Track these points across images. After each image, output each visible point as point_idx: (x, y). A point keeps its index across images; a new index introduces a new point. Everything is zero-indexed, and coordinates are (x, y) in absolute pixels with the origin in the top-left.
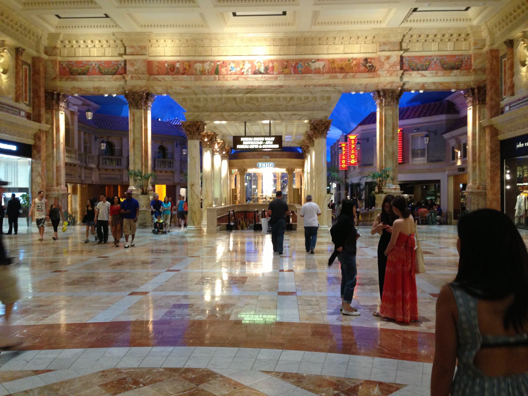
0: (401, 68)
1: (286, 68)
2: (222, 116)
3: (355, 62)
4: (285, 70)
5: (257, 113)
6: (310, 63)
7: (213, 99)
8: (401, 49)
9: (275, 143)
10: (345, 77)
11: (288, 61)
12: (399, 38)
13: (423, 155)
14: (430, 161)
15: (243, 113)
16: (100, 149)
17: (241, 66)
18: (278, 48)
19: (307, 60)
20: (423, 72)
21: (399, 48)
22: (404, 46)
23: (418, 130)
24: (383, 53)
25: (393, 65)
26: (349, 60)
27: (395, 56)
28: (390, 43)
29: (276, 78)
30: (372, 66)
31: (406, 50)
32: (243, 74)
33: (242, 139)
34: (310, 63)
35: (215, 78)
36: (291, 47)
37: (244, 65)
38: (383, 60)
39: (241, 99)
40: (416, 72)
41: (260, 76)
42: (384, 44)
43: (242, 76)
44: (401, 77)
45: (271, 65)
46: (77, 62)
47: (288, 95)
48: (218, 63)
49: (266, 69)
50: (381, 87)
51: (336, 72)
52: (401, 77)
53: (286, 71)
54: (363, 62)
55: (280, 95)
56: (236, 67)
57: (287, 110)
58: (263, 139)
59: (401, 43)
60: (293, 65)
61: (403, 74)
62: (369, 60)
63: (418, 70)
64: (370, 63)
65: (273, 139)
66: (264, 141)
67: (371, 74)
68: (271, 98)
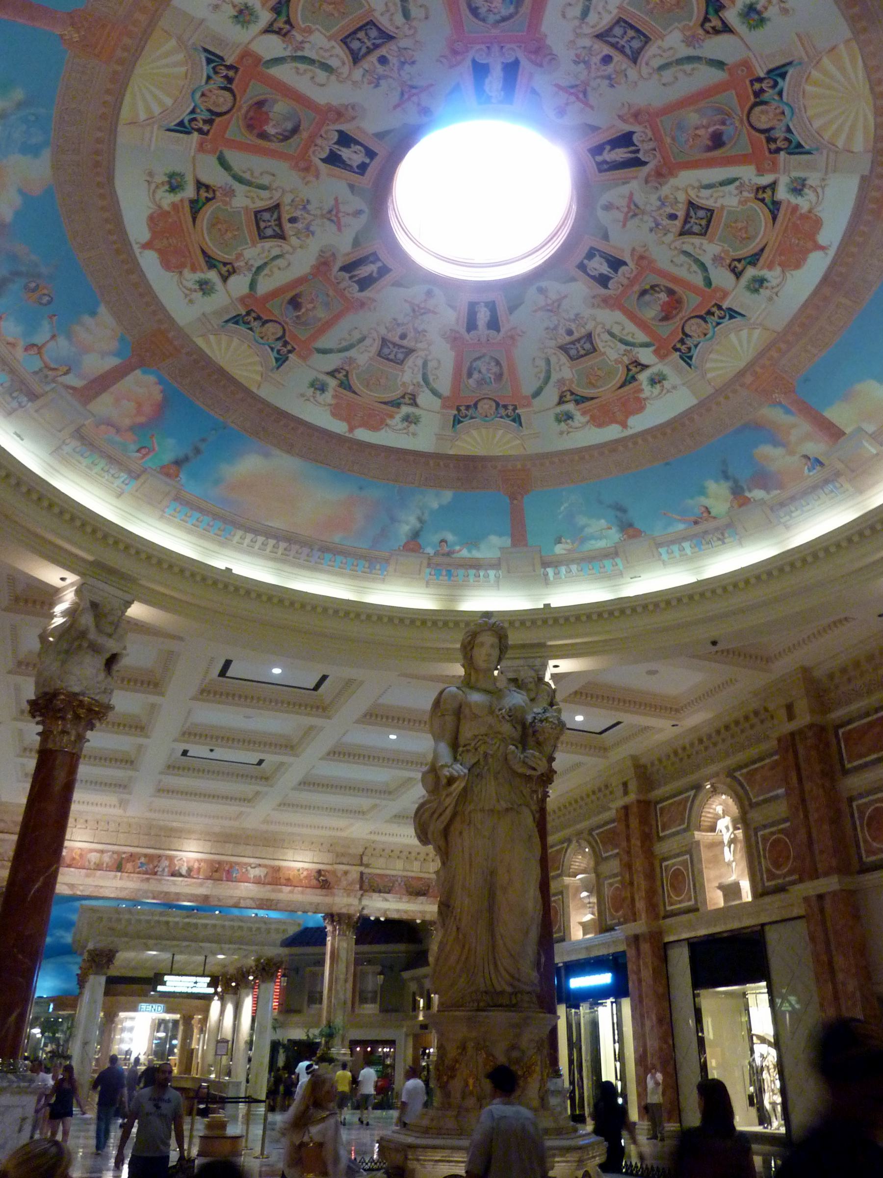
0: (361, 888)
1: (216, 871)
2: (145, 944)
3: (305, 873)
4: (214, 874)
5: (193, 944)
6: (249, 868)
7: (139, 921)
8: (361, 864)
9: (209, 985)
10: (291, 892)
11: (219, 863)
12: (361, 850)
13: (374, 1001)
14: (384, 1010)
15: (175, 943)
17: (156, 863)
18: (210, 844)
19: (246, 864)
20: (386, 895)
21: (359, 862)
23: (369, 962)
24: (341, 866)
25: (351, 884)
26: (299, 870)
27: (355, 872)
28: (350, 854)
29: (201, 885)
30: (326, 881)
31: (367, 866)
32: (156, 874)
33: (166, 978)
34: (249, 868)
35: (116, 876)
36: (227, 845)
37: (159, 861)
38: (339, 875)
39: (177, 923)
40: (377, 894)
41: (180, 879)
42: (343, 855)
43: (156, 877)
45: (196, 865)
47: (236, 924)
48: (124, 856)
49: (190, 870)
50: (335, 910)
51: (280, 885)
52: (360, 900)
53: (216, 875)
54: (316, 874)
55: (227, 923)
56: (148, 864)
57: (231, 943)
58: (194, 979)
60: (227, 868)
61: (362, 895)
62: (323, 873)
63: (380, 892)
64: (324, 876)
65: (208, 980)
66: (196, 983)
67: (324, 891)
68: (214, 926)
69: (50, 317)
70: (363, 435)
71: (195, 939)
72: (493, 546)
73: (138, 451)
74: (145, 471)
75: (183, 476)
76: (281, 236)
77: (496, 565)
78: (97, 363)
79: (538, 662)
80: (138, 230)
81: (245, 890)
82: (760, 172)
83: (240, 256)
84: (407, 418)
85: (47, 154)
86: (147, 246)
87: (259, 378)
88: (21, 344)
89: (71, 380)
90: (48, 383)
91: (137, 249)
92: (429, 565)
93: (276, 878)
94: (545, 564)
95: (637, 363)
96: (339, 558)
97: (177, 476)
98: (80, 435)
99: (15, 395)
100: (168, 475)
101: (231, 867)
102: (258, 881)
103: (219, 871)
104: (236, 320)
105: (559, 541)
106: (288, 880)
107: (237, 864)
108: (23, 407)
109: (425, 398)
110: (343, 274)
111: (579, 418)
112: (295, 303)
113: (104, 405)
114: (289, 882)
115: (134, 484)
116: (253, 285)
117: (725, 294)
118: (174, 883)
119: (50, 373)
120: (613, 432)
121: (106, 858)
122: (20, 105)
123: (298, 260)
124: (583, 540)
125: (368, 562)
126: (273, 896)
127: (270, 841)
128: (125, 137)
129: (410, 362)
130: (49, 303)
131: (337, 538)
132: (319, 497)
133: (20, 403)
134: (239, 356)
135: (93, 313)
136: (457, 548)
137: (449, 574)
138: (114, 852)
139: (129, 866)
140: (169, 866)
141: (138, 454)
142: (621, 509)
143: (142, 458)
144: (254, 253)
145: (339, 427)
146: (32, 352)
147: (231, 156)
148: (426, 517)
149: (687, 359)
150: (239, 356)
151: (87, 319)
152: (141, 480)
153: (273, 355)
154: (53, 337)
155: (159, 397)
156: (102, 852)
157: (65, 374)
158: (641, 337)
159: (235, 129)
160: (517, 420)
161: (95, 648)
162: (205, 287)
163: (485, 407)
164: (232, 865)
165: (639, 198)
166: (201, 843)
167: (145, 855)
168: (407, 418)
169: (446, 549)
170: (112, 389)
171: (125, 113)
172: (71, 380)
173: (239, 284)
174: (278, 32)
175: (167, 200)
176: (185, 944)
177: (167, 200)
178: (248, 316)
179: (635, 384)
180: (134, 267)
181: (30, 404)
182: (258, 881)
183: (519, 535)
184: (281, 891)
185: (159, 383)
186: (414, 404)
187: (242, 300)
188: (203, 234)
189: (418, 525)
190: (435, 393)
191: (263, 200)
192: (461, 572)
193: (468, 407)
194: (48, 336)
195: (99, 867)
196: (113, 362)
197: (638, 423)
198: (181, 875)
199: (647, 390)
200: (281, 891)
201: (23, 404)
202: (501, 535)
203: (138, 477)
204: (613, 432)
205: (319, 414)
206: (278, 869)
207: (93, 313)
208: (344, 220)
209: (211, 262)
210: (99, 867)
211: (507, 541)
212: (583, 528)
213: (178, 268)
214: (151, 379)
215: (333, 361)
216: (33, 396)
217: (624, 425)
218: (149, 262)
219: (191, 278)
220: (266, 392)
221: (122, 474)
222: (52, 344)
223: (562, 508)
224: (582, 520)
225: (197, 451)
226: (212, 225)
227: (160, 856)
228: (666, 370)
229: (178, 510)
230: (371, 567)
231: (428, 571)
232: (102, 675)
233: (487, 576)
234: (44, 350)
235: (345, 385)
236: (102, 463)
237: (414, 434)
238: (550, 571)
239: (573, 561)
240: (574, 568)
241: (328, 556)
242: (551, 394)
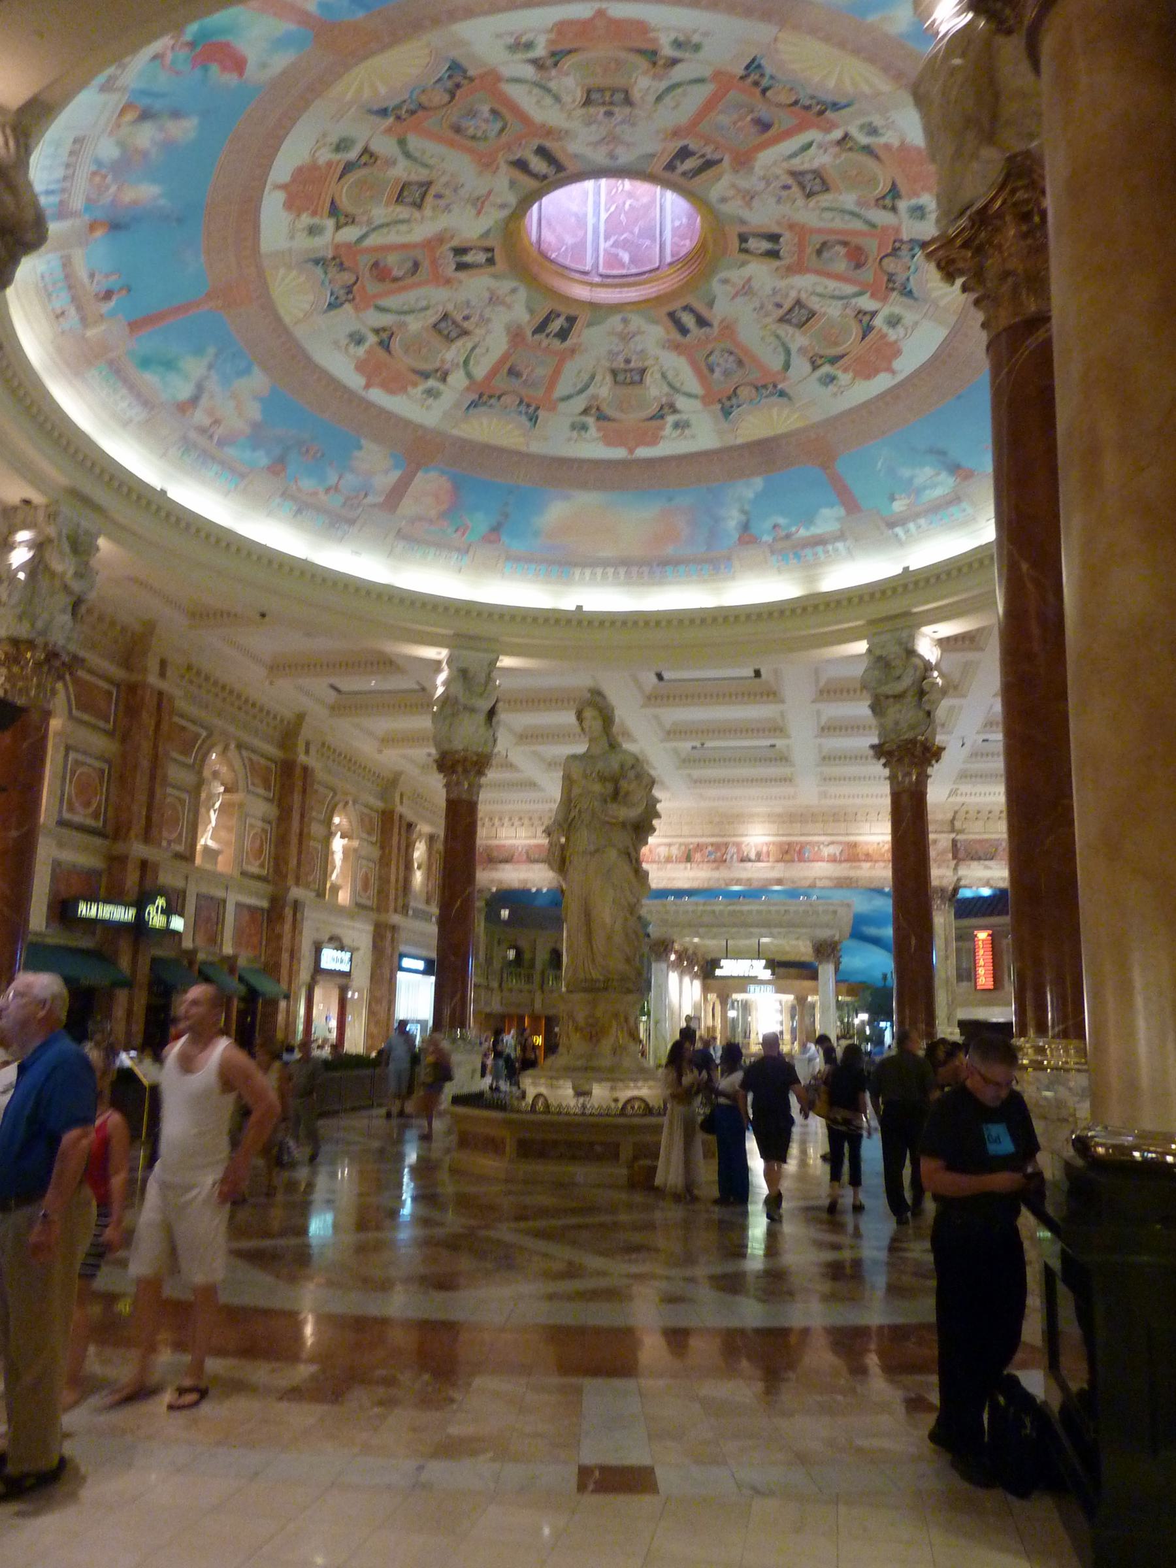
0: (955, 857)
1: (787, 852)
8: (953, 830)
11: (789, 844)
12: (950, 816)
15: (724, 929)
16: (505, 957)
20: (987, 863)
22: (958, 824)
25: (943, 852)
29: (773, 868)
31: (961, 832)
39: (721, 912)
41: (750, 864)
44: (955, 869)
45: (765, 849)
46: (497, 846)
53: (787, 857)
55: (773, 908)
59: (952, 821)
63: (980, 859)
70: (643, 452)
71: (745, 925)
72: (828, 519)
73: (456, 531)
75: (505, 539)
76: (465, 333)
77: (841, 536)
78: (386, 479)
79: (904, 634)
80: (355, 381)
81: (819, 870)
82: (828, 131)
83: (443, 361)
84: (676, 425)
86: (368, 386)
87: (522, 439)
88: (321, 490)
89: (370, 499)
91: (363, 393)
92: (773, 552)
93: (852, 854)
94: (891, 525)
95: (860, 313)
96: (681, 568)
98: (400, 535)
100: (491, 542)
101: (802, 848)
102: (833, 860)
103: (790, 853)
104: (474, 404)
105: (892, 499)
106: (867, 855)
107: (808, 843)
109: (681, 402)
110: (537, 337)
111: (844, 378)
112: (513, 372)
113: (408, 507)
114: (868, 857)
116: (469, 375)
117: (897, 230)
118: (745, 869)
120: (882, 382)
121: (675, 851)
122: (216, 355)
123: (493, 344)
124: (918, 491)
125: (712, 563)
126: (853, 873)
127: (840, 817)
128: (300, 332)
129: (648, 379)
130: (323, 455)
131: (670, 550)
132: (635, 519)
134: (495, 429)
136: (794, 529)
137: (797, 556)
138: (681, 845)
139: (698, 856)
140: (738, 852)
142: (942, 453)
144: (453, 353)
145: (619, 453)
147: (386, 302)
148: (747, 507)
149: (908, 293)
150: (495, 429)
151: (357, 453)
152: (471, 553)
153: (524, 419)
154: (340, 478)
156: (670, 845)
157: (366, 495)
158: (849, 289)
159: (372, 287)
160: (782, 394)
161: (472, 710)
162: (431, 393)
163: (744, 392)
164: (803, 846)
165: (744, 183)
166: (767, 825)
167: (712, 845)
168: (676, 425)
169: (783, 533)
171: (287, 320)
173: (458, 379)
174: (346, 224)
175: (361, 351)
176: (734, 930)
177: (361, 351)
178: (482, 397)
179: (874, 332)
180: (369, 405)
182: (833, 860)
183: (849, 502)
184: (860, 868)
186: (675, 411)
187: (468, 389)
188: (403, 360)
189: (743, 518)
190: (689, 395)
191: (432, 317)
192: (808, 552)
193: (729, 398)
195: (668, 860)
196: (395, 475)
197: (908, 362)
198: (750, 860)
199: (892, 335)
200: (860, 868)
202: (832, 506)
203: (467, 552)
204: (882, 382)
205: (592, 448)
206: (855, 845)
207: (360, 448)
208: (508, 299)
209: (426, 375)
210: (668, 860)
211: (840, 511)
212: (911, 479)
213: (403, 389)
214: (433, 474)
215: (580, 403)
216: (351, 522)
217: (893, 372)
218: (377, 396)
219: (418, 391)
220: (536, 447)
222: (342, 482)
223: (879, 464)
224: (906, 473)
225: (506, 516)
226: (406, 351)
227: (726, 845)
228: (897, 310)
230: (716, 569)
231: (774, 558)
232: (482, 730)
233: (836, 550)
235: (601, 417)
236: (432, 550)
237: (693, 437)
238: (899, 530)
239: (917, 516)
240: (922, 521)
241: (669, 569)
242: (801, 366)
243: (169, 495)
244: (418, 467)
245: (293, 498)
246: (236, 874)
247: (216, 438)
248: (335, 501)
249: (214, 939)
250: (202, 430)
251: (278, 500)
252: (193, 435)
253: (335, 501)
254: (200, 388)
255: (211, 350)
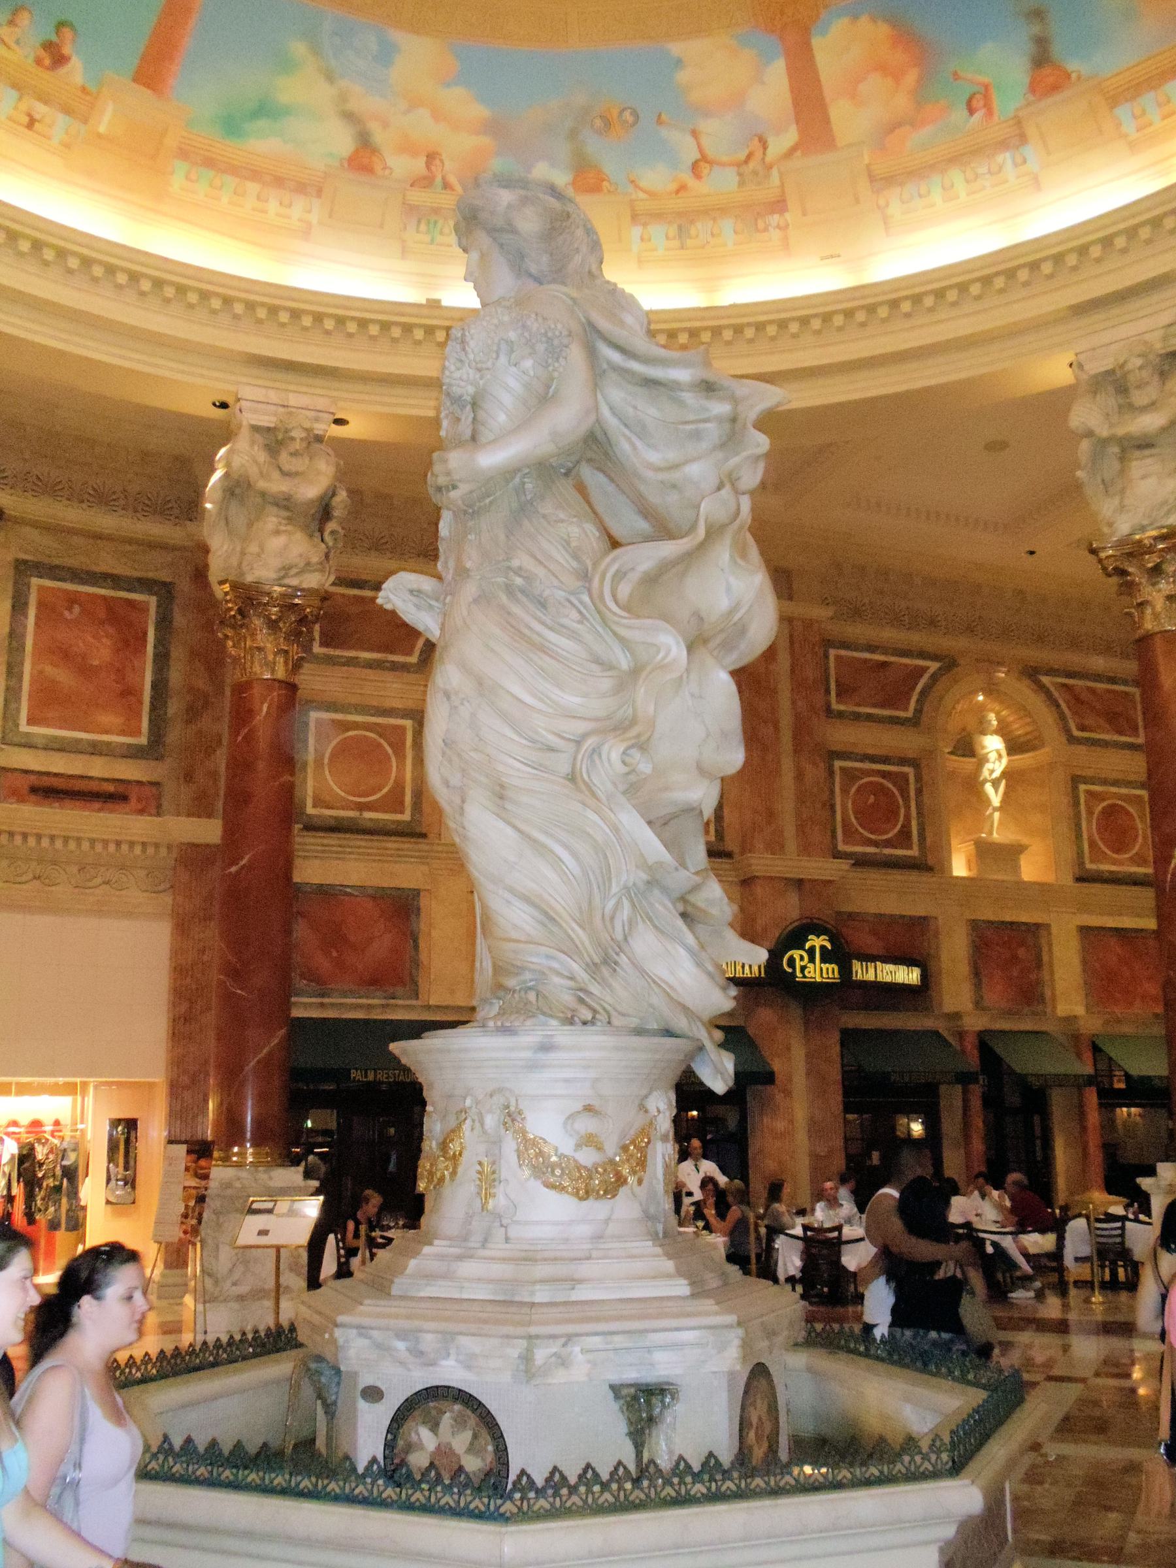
69: (659, 121)
73: (971, 111)
74: (1018, 122)
75: (1073, 66)
85: (398, 36)
88: (687, 177)
89: (780, 144)
90: (767, 176)
97: (1068, 76)
99: (761, 224)
100: (1055, 88)
108: (787, 226)
113: (850, 120)
115: (1029, 151)
119: (751, 165)
133: (778, 227)
135: (679, 63)
141: (978, 116)
143: (990, 112)
146: (706, 172)
151: (683, 76)
154: (695, 134)
155: (883, 29)
170: (828, 93)
172: (780, 144)
181: (787, 215)
185: (855, 17)
194: (689, 140)
196: (778, 72)
201: (782, 224)
207: (679, 63)
216: (779, 205)
221: (1000, 158)
229: (1138, 112)
234: (710, 153)
236: (956, 176)
243: (444, 303)
244: (805, 33)
245: (658, 216)
246: (1068, 880)
247: (452, 179)
248: (721, 183)
249: (1030, 993)
250: (424, 182)
251: (636, 231)
252: (418, 197)
253: (721, 183)
254: (349, 117)
255: (299, 48)
